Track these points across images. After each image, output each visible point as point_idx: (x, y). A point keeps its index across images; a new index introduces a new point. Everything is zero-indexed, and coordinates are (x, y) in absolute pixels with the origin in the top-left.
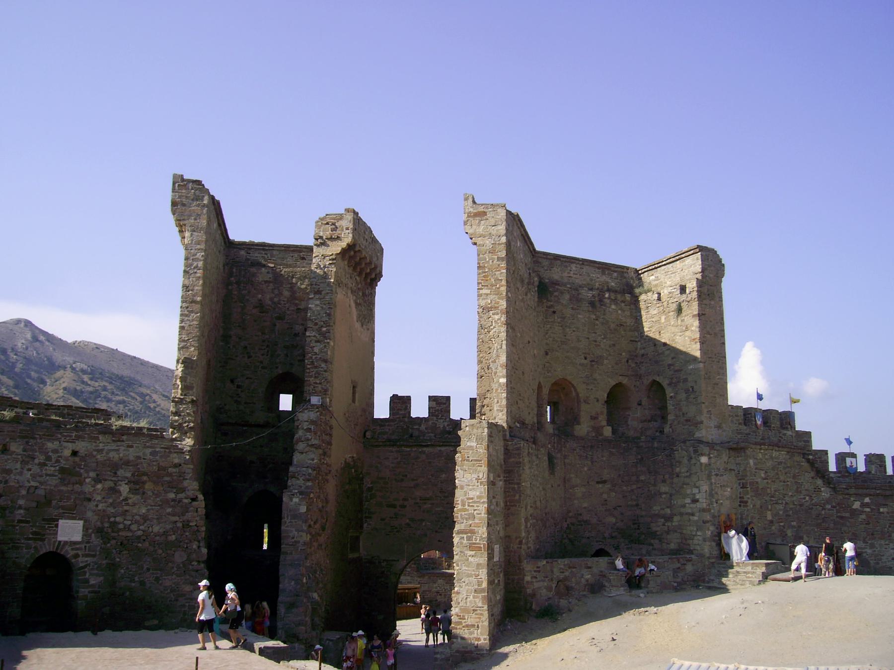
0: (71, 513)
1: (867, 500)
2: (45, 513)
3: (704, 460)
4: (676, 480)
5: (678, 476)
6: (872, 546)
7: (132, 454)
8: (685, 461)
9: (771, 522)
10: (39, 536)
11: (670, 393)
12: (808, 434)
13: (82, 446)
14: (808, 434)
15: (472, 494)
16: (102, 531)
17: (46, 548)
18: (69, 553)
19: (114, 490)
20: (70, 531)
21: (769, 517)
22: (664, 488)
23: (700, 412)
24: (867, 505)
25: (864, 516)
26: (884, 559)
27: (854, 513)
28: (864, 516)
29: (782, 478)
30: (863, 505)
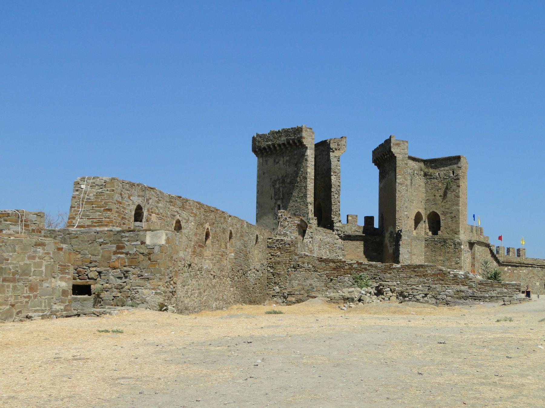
1: (510, 267)
3: (462, 247)
4: (447, 255)
5: (448, 253)
7: (328, 240)
8: (453, 246)
11: (442, 218)
12: (488, 237)
14: (488, 237)
15: (405, 257)
19: (326, 252)
22: (440, 258)
23: (459, 228)
28: (508, 274)
30: (509, 269)
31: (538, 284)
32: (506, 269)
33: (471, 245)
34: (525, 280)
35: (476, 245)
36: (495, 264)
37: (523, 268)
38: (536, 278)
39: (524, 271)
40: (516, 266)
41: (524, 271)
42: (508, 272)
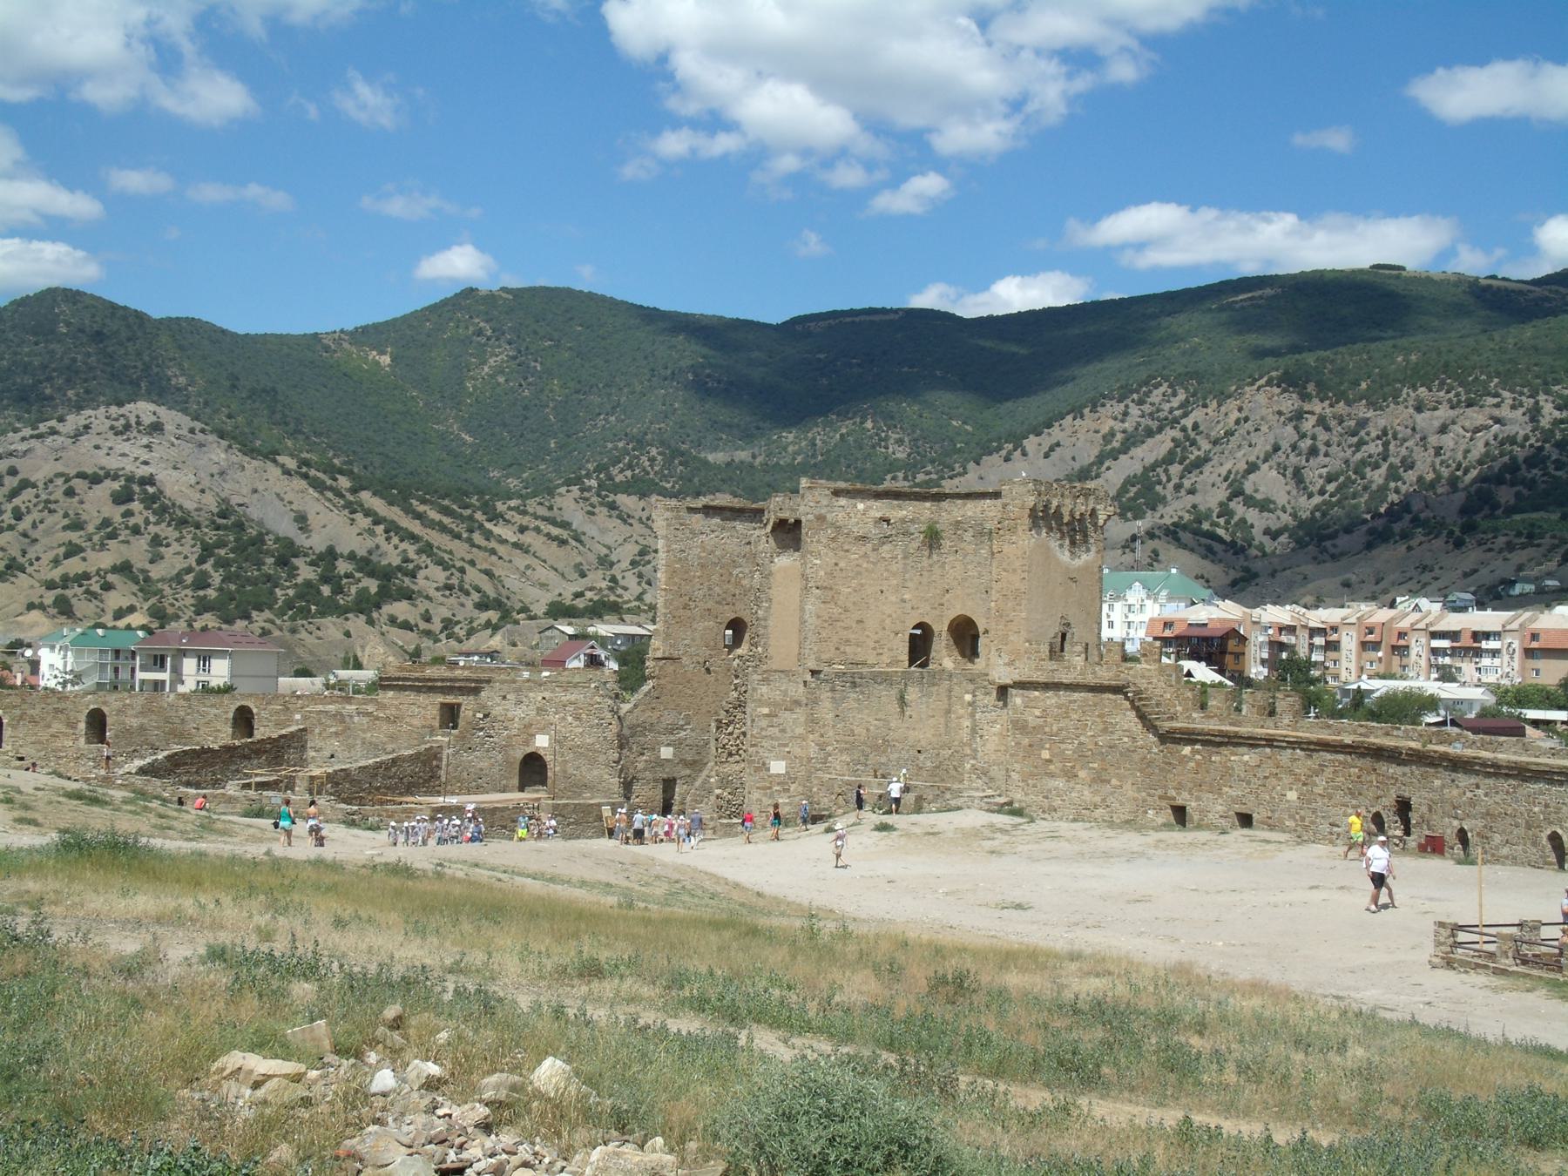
0: (542, 730)
2: (528, 731)
6: (1198, 799)
7: (573, 698)
9: (1050, 761)
10: (527, 743)
13: (547, 695)
16: (558, 741)
17: (529, 750)
18: (542, 753)
19: (564, 719)
20: (542, 742)
21: (1046, 755)
24: (1198, 752)
25: (1192, 764)
26: (1210, 816)
27: (1183, 760)
28: (1192, 764)
29: (1074, 716)
30: (1194, 752)
31: (1292, 796)
32: (1187, 750)
33: (1003, 691)
34: (1249, 783)
35: (1014, 691)
36: (1152, 738)
37: (1245, 749)
38: (1287, 779)
39: (1246, 758)
40: (1220, 744)
41: (1248, 757)
42: (1191, 759)
